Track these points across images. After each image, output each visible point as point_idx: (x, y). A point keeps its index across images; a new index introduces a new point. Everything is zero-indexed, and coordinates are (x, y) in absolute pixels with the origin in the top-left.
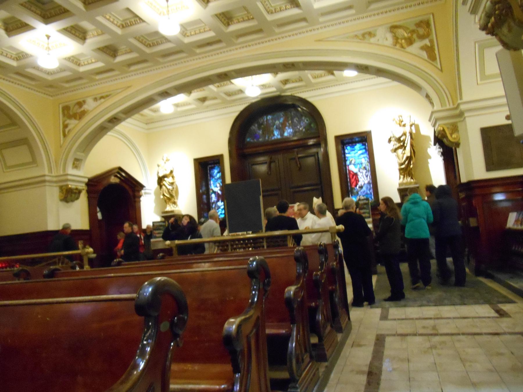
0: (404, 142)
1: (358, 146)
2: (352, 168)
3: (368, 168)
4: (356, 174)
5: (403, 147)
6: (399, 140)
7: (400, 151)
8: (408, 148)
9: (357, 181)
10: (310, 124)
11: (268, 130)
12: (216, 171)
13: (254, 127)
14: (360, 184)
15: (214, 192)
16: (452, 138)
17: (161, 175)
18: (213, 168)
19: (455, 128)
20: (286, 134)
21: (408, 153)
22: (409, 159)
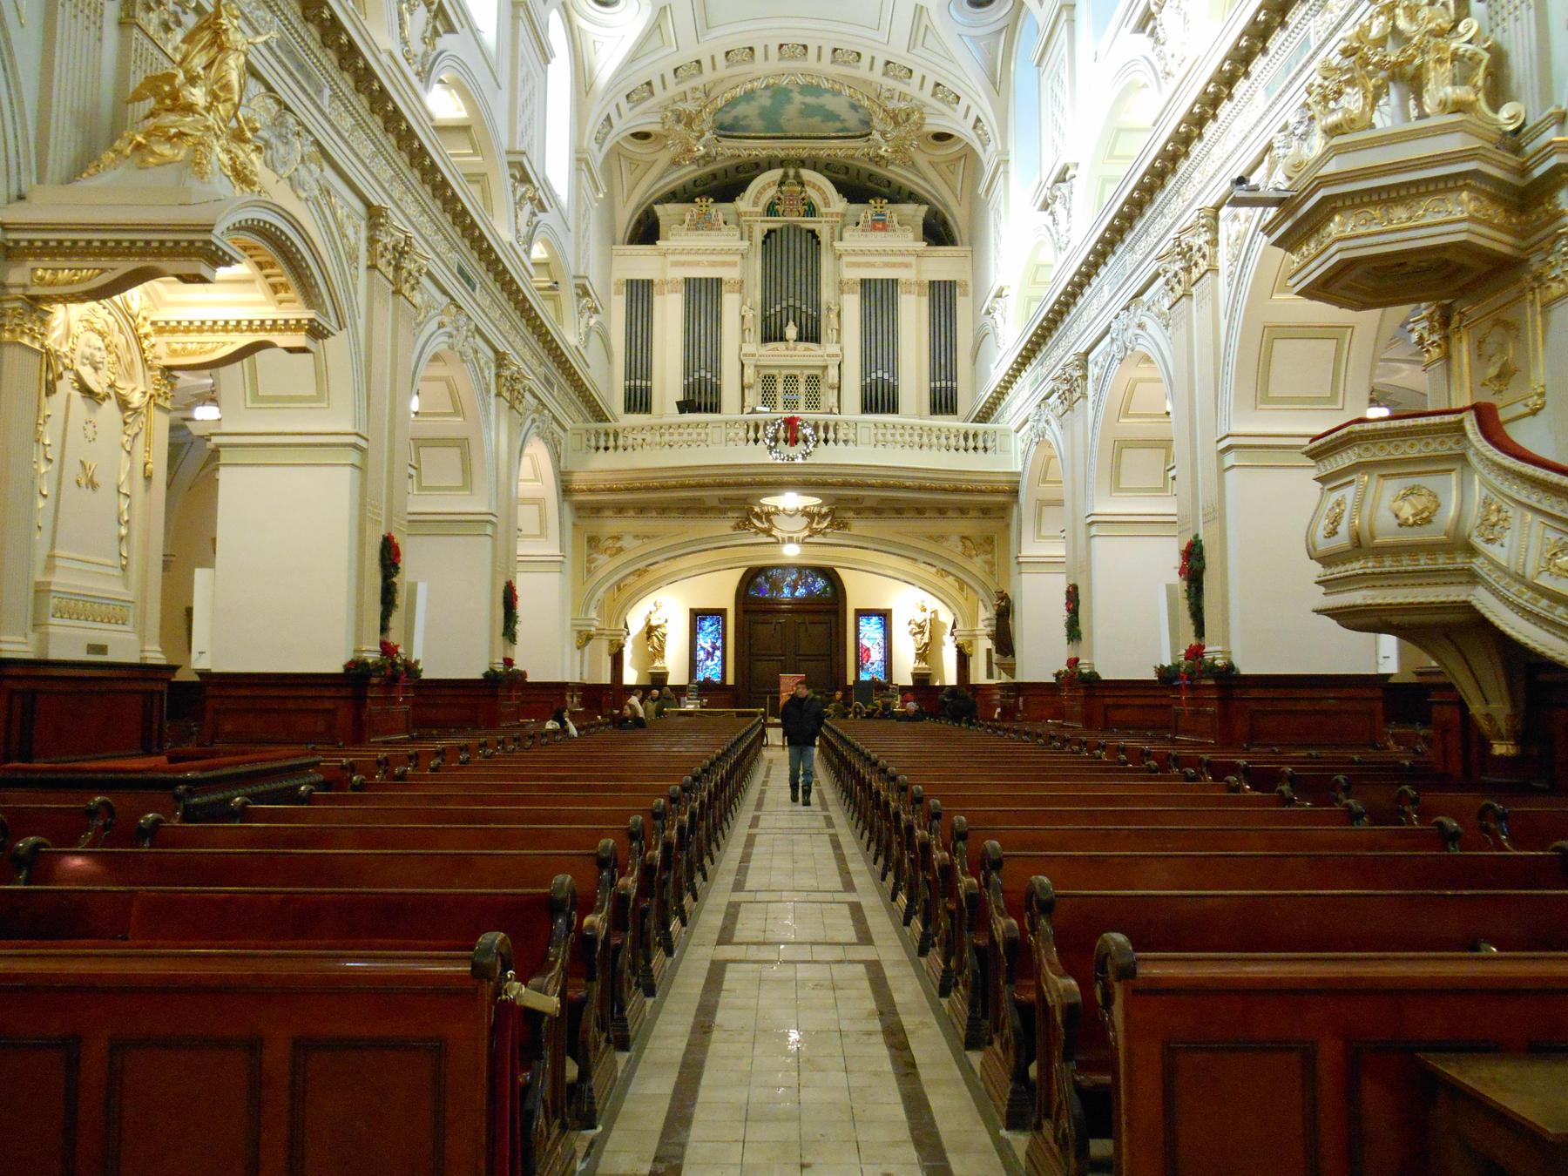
0: (923, 627)
1: (875, 619)
2: (865, 642)
3: (882, 644)
4: (868, 649)
5: (922, 633)
6: (919, 626)
7: (919, 636)
8: (927, 635)
9: (869, 656)
10: (825, 587)
11: (776, 586)
12: (707, 624)
13: (760, 580)
14: (871, 660)
15: (702, 648)
16: (967, 650)
17: (654, 623)
18: (704, 619)
19: (970, 644)
20: (797, 594)
21: (926, 639)
22: (926, 645)
